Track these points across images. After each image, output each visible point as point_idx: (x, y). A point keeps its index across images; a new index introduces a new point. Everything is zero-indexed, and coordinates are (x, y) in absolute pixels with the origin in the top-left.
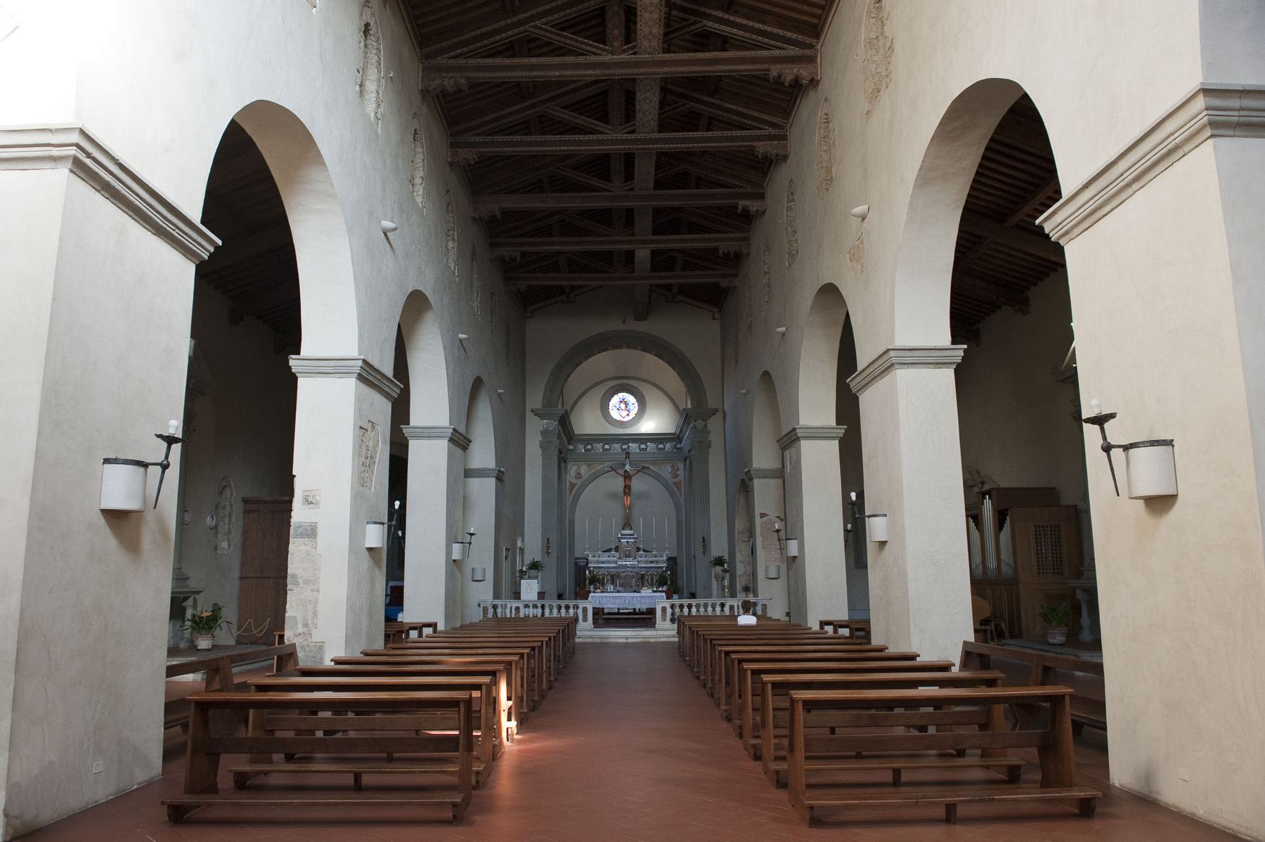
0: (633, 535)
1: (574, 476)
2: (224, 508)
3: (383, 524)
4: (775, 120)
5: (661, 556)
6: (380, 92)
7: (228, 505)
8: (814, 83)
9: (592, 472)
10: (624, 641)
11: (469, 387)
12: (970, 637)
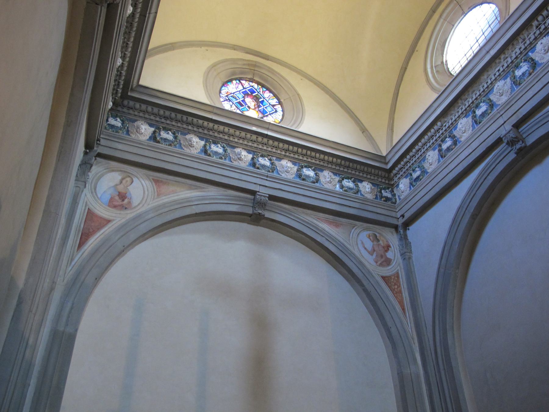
1: (107, 197)
9: (165, 199)
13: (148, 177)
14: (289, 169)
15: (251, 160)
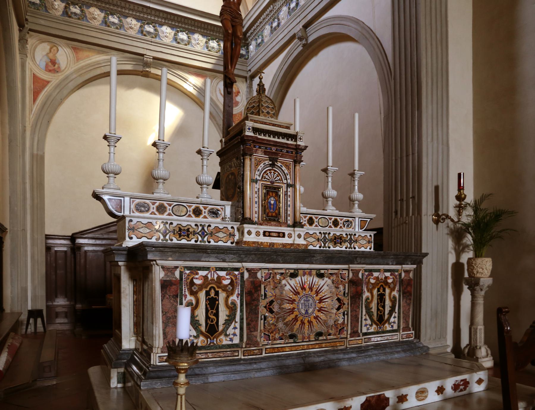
13: (68, 45)
14: (168, 35)
15: (139, 28)
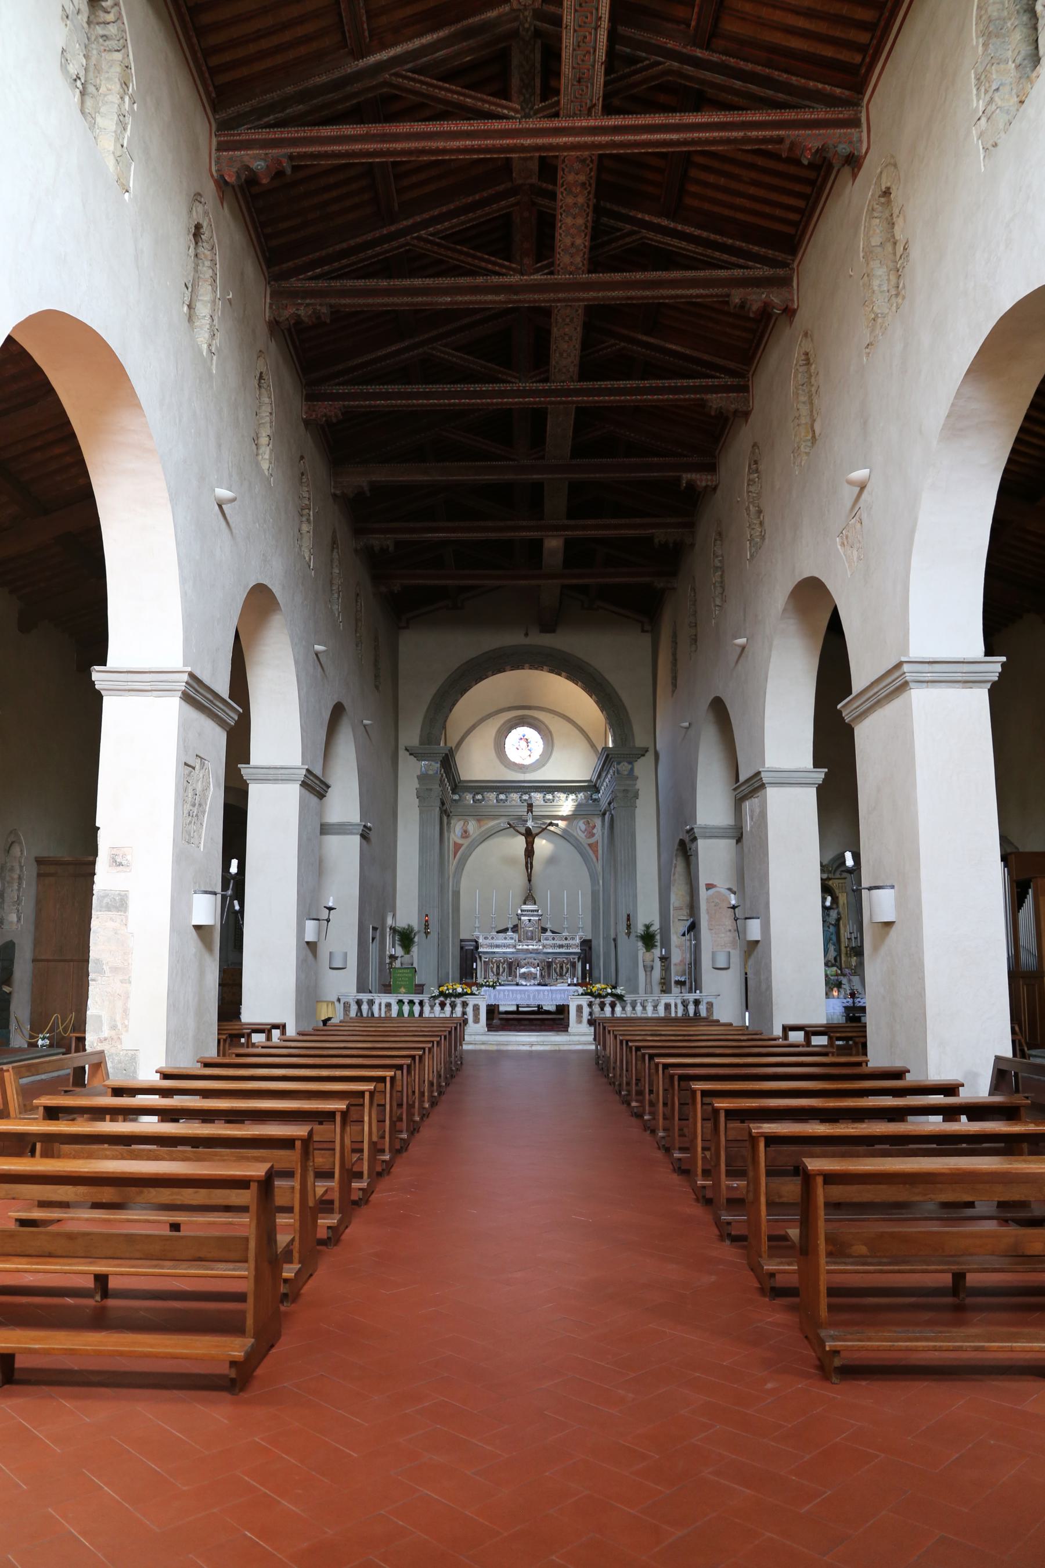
0: (537, 911)
2: (12, 869)
3: (215, 894)
4: (732, 365)
5: (573, 939)
6: (216, 318)
7: (17, 867)
8: (790, 312)
9: (483, 829)
10: (527, 1048)
11: (327, 715)
12: (1008, 1052)
